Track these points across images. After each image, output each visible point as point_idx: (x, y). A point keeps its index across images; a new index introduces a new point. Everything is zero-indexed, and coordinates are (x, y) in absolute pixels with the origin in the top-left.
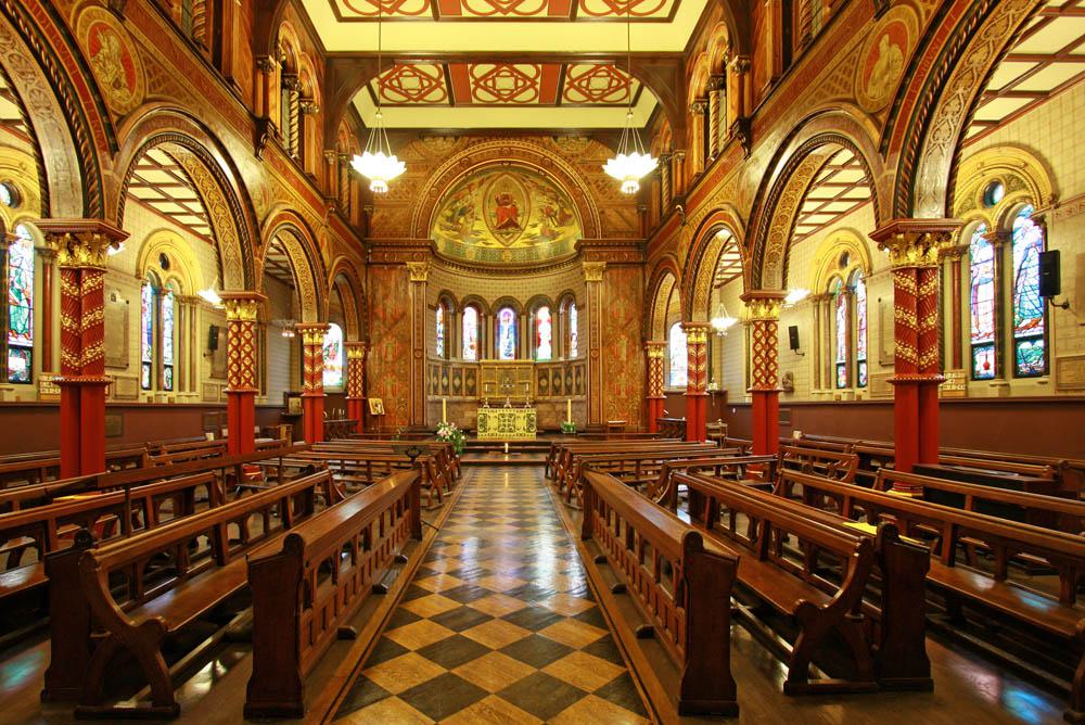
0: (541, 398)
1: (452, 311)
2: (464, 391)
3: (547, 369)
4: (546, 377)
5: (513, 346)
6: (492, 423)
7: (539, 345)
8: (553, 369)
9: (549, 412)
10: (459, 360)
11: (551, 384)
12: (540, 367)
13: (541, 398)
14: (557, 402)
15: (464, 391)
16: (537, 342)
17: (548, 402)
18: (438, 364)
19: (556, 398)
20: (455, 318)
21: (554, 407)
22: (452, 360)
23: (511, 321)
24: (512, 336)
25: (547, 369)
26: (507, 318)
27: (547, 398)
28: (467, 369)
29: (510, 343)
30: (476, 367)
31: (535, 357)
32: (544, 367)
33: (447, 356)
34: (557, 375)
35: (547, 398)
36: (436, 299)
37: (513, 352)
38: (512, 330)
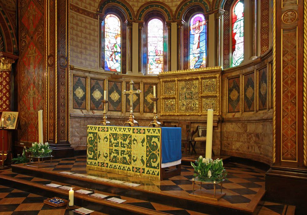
0: (230, 115)
1: (126, 22)
2: (142, 109)
3: (238, 77)
4: (237, 87)
5: (204, 56)
6: (103, 147)
7: (234, 50)
8: (246, 75)
9: (239, 134)
10: (135, 73)
11: (242, 96)
12: (229, 75)
13: (230, 115)
14: (249, 121)
15: (142, 109)
16: (230, 45)
17: (237, 121)
18: (102, 77)
19: (247, 115)
20: (131, 30)
21: (245, 128)
22: (128, 73)
23: (203, 28)
24: (203, 44)
25: (238, 77)
26: (197, 24)
27: (237, 115)
28: (145, 84)
29: (201, 53)
30: (156, 81)
31: (226, 64)
32: (234, 74)
33: (124, 70)
34: (249, 83)
35: (237, 115)
36: (97, 5)
37: (204, 62)
38: (204, 37)
